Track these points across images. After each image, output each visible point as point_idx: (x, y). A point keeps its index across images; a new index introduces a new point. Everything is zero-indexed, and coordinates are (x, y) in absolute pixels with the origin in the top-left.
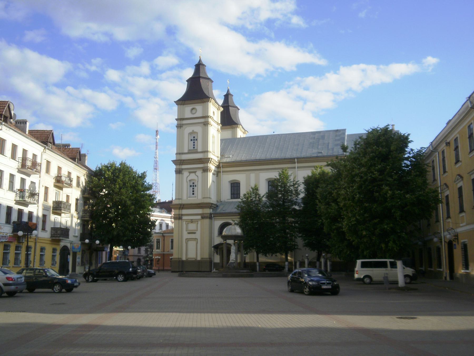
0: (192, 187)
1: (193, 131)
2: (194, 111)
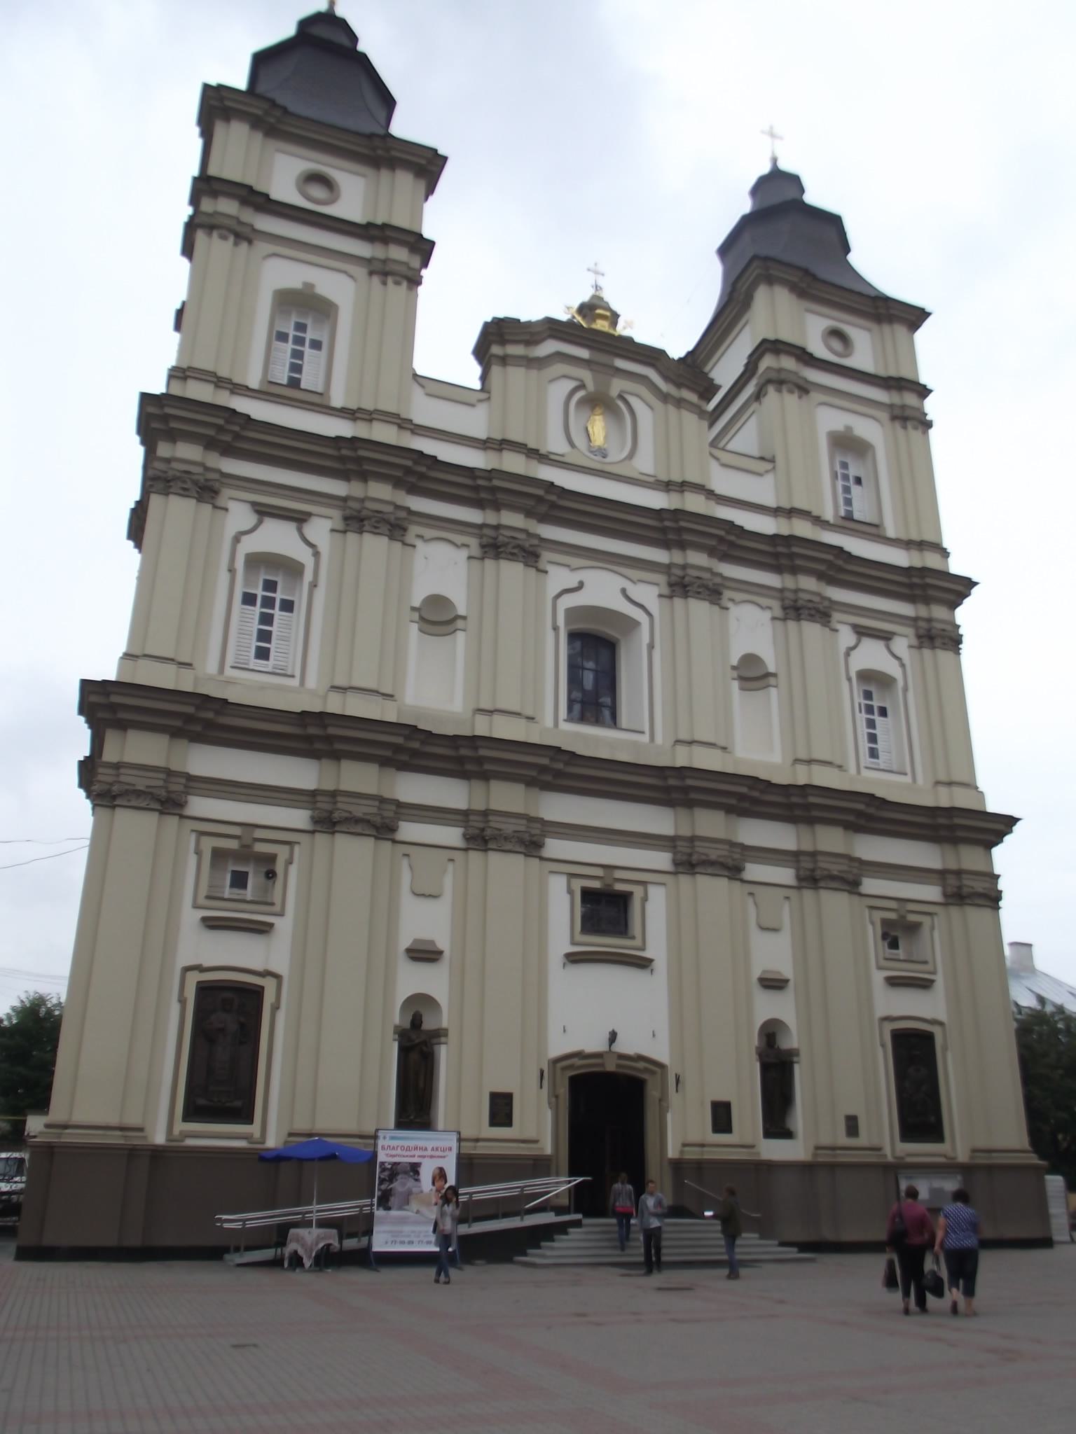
0: (258, 609)
1: (309, 286)
2: (318, 192)
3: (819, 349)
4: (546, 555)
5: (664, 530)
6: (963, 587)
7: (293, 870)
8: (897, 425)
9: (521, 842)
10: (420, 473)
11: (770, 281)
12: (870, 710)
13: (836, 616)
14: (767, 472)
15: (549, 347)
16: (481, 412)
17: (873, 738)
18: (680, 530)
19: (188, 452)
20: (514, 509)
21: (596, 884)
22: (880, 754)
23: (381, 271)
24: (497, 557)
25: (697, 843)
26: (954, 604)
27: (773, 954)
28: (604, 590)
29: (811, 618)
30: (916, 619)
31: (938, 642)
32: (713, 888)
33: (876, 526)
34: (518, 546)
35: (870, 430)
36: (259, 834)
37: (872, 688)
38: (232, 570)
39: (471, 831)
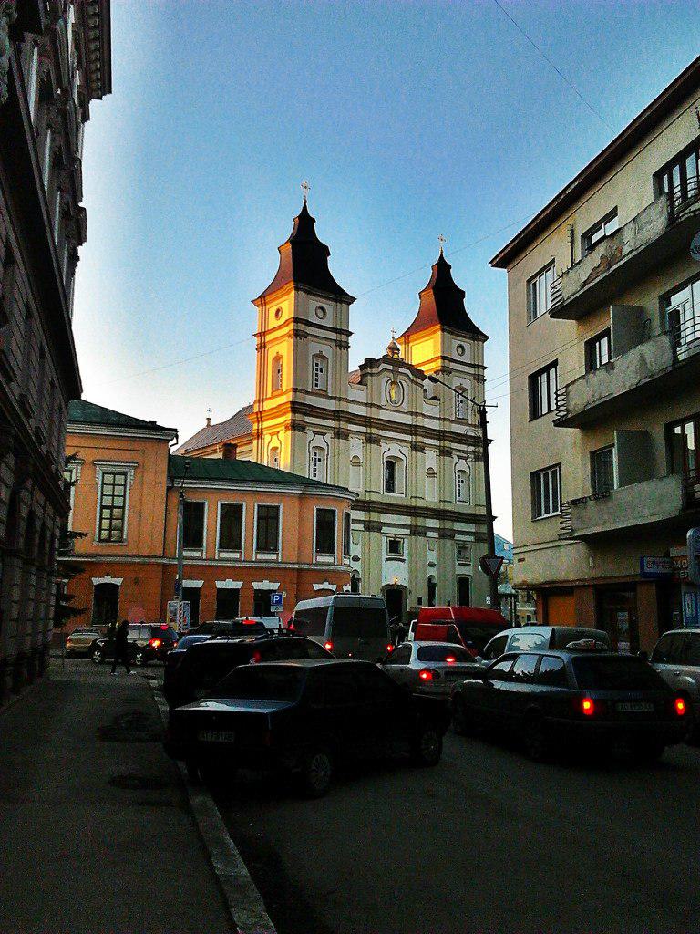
10: (353, 419)
12: (459, 481)
15: (383, 366)
19: (298, 417)
24: (370, 443)
27: (432, 557)
28: (394, 450)
32: (420, 539)
35: (467, 384)
37: (460, 474)
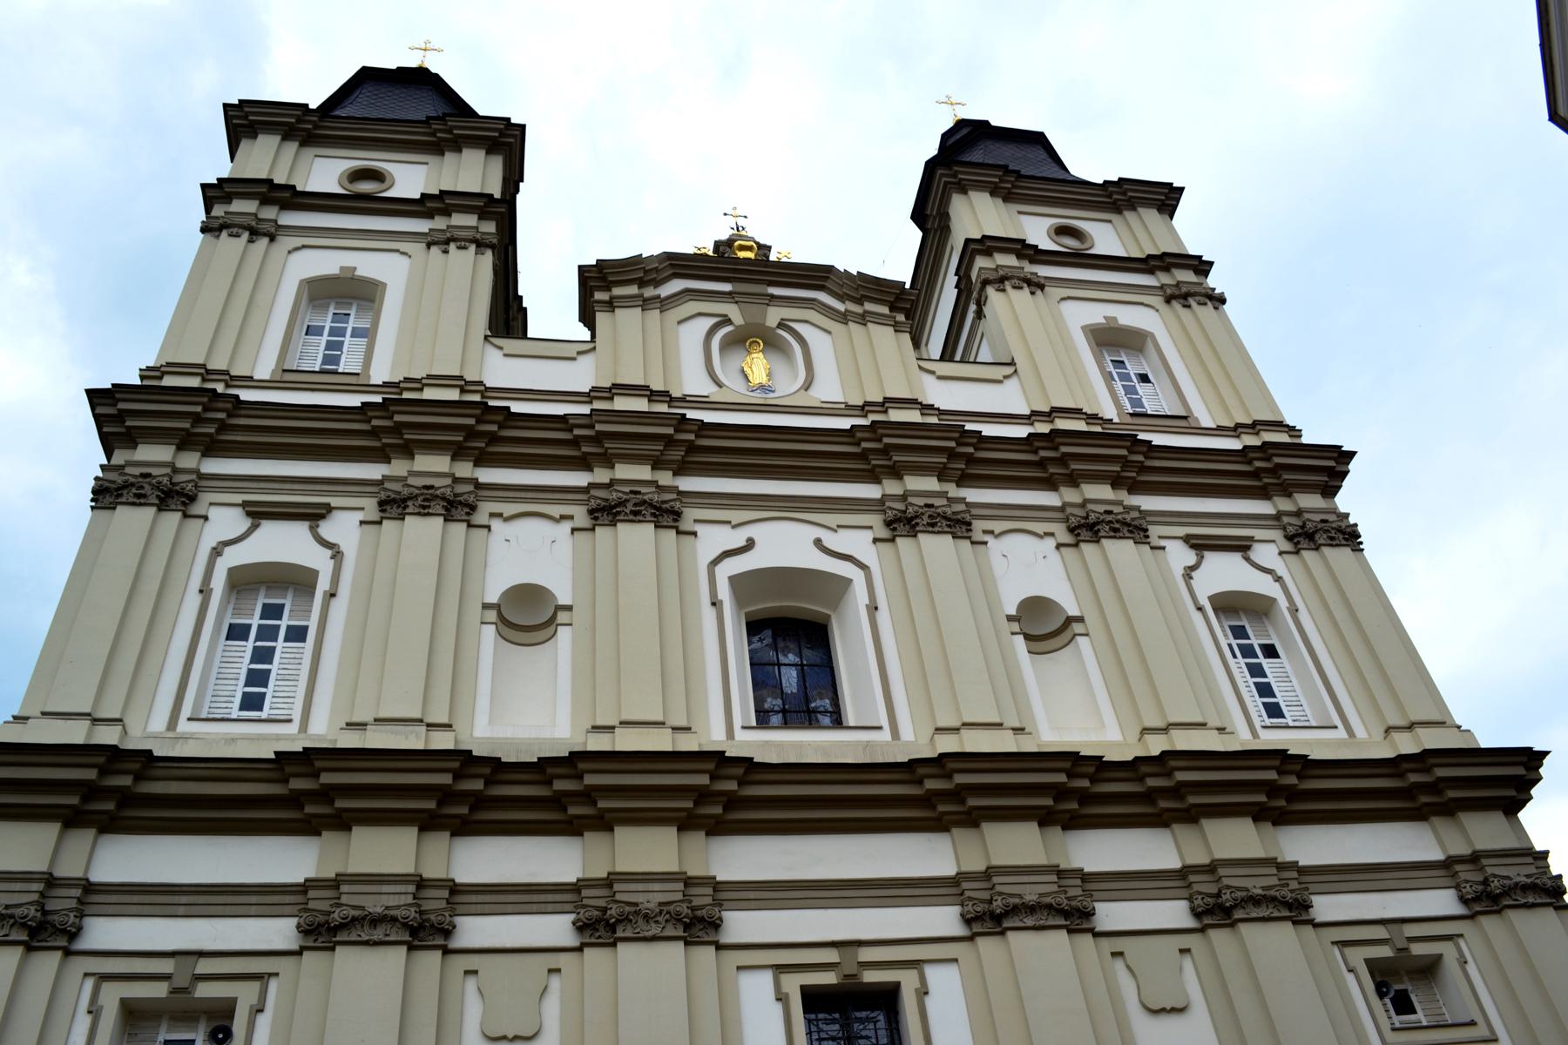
0: (250, 645)
3: (1046, 244)
4: (690, 514)
5: (863, 456)
6: (1331, 465)
7: (264, 1022)
8: (1176, 305)
9: (677, 919)
11: (964, 191)
12: (1248, 652)
13: (1155, 531)
14: (1006, 377)
16: (586, 362)
17: (1265, 690)
18: (886, 451)
20: (638, 459)
21: (829, 978)
22: (1285, 710)
23: (440, 241)
24: (613, 524)
25: (996, 880)
26: (1330, 491)
28: (785, 545)
29: (1115, 533)
30: (1278, 516)
31: (1321, 538)
32: (1042, 953)
33: (1185, 418)
34: (644, 502)
36: (204, 967)
38: (205, 591)
39: (584, 915)
